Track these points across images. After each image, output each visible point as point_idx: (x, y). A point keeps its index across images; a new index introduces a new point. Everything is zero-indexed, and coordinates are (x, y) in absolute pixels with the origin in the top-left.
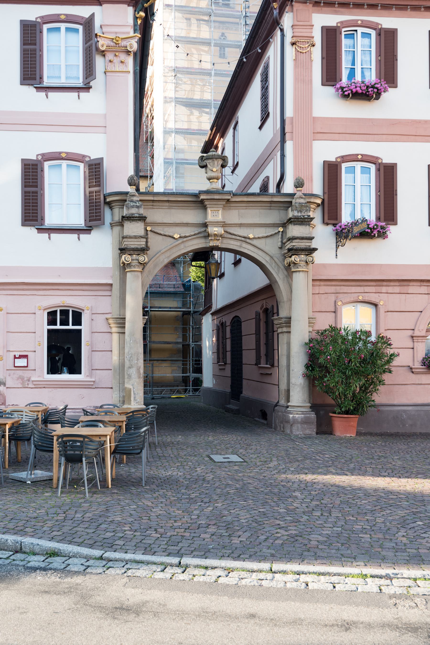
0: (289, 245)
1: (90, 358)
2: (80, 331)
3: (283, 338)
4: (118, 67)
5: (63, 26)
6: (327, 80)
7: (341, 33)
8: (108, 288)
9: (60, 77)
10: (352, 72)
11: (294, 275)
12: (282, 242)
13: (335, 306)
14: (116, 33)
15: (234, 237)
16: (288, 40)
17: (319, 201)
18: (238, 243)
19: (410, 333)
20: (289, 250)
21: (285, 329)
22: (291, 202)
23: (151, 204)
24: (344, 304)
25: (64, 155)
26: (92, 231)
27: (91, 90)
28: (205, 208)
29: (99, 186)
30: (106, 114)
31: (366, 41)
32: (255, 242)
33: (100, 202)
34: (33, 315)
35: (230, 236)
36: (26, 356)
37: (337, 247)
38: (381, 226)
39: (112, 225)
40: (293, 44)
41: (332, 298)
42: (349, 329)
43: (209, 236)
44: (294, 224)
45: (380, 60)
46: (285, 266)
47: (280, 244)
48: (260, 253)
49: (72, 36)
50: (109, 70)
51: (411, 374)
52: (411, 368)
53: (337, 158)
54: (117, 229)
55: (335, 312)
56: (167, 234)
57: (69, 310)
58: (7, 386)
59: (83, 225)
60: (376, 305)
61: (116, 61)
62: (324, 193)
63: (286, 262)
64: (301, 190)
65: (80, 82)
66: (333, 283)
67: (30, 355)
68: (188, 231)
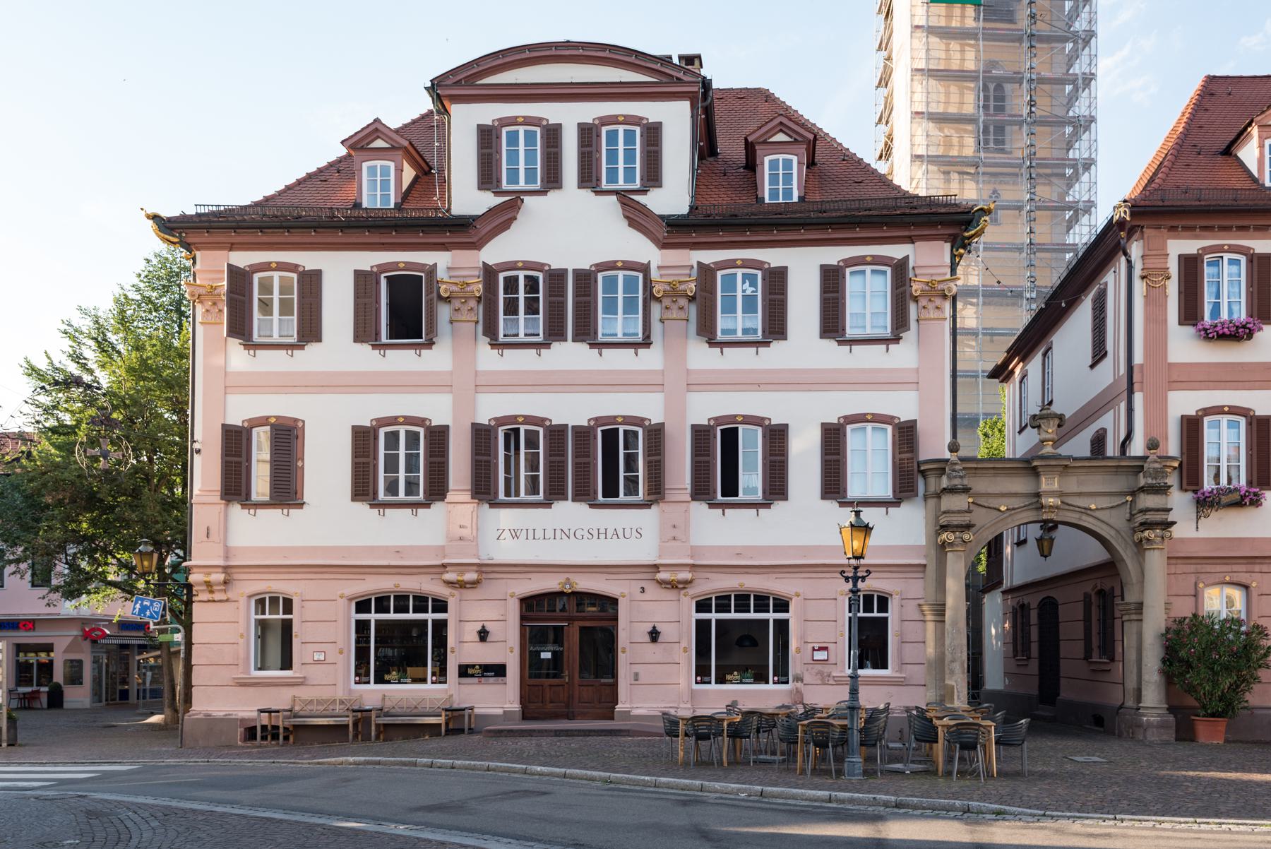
0: (1140, 518)
1: (900, 652)
2: (886, 619)
3: (1131, 629)
4: (933, 314)
5: (868, 269)
6: (1186, 319)
7: (1203, 262)
8: (919, 569)
9: (864, 327)
10: (1216, 308)
11: (1147, 553)
12: (1130, 513)
13: (1196, 588)
14: (932, 275)
15: (1072, 508)
16: (1137, 272)
17: (1176, 464)
18: (1077, 516)
20: (1142, 524)
21: (1134, 617)
22: (1143, 466)
23: (974, 471)
24: (1207, 586)
25: (869, 417)
26: (902, 505)
27: (901, 341)
29: (912, 452)
30: (918, 369)
31: (1234, 269)
32: (1097, 514)
33: (913, 470)
34: (834, 601)
35: (1067, 507)
36: (826, 649)
37: (1198, 518)
38: (1254, 493)
39: (926, 498)
40: (1143, 278)
41: (1192, 579)
42: (1214, 616)
43: (1042, 507)
44: (1148, 494)
45: (1252, 292)
46: (1134, 542)
47: (1128, 515)
48: (1104, 526)
49: (879, 279)
50: (923, 317)
53: (1197, 411)
54: (932, 502)
55: (1195, 596)
56: (991, 505)
58: (805, 682)
59: (891, 497)
60: (1246, 587)
61: (930, 306)
62: (1182, 454)
63: (1135, 538)
64: (1154, 453)
66: (1193, 561)
67: (831, 646)
68: (1015, 502)
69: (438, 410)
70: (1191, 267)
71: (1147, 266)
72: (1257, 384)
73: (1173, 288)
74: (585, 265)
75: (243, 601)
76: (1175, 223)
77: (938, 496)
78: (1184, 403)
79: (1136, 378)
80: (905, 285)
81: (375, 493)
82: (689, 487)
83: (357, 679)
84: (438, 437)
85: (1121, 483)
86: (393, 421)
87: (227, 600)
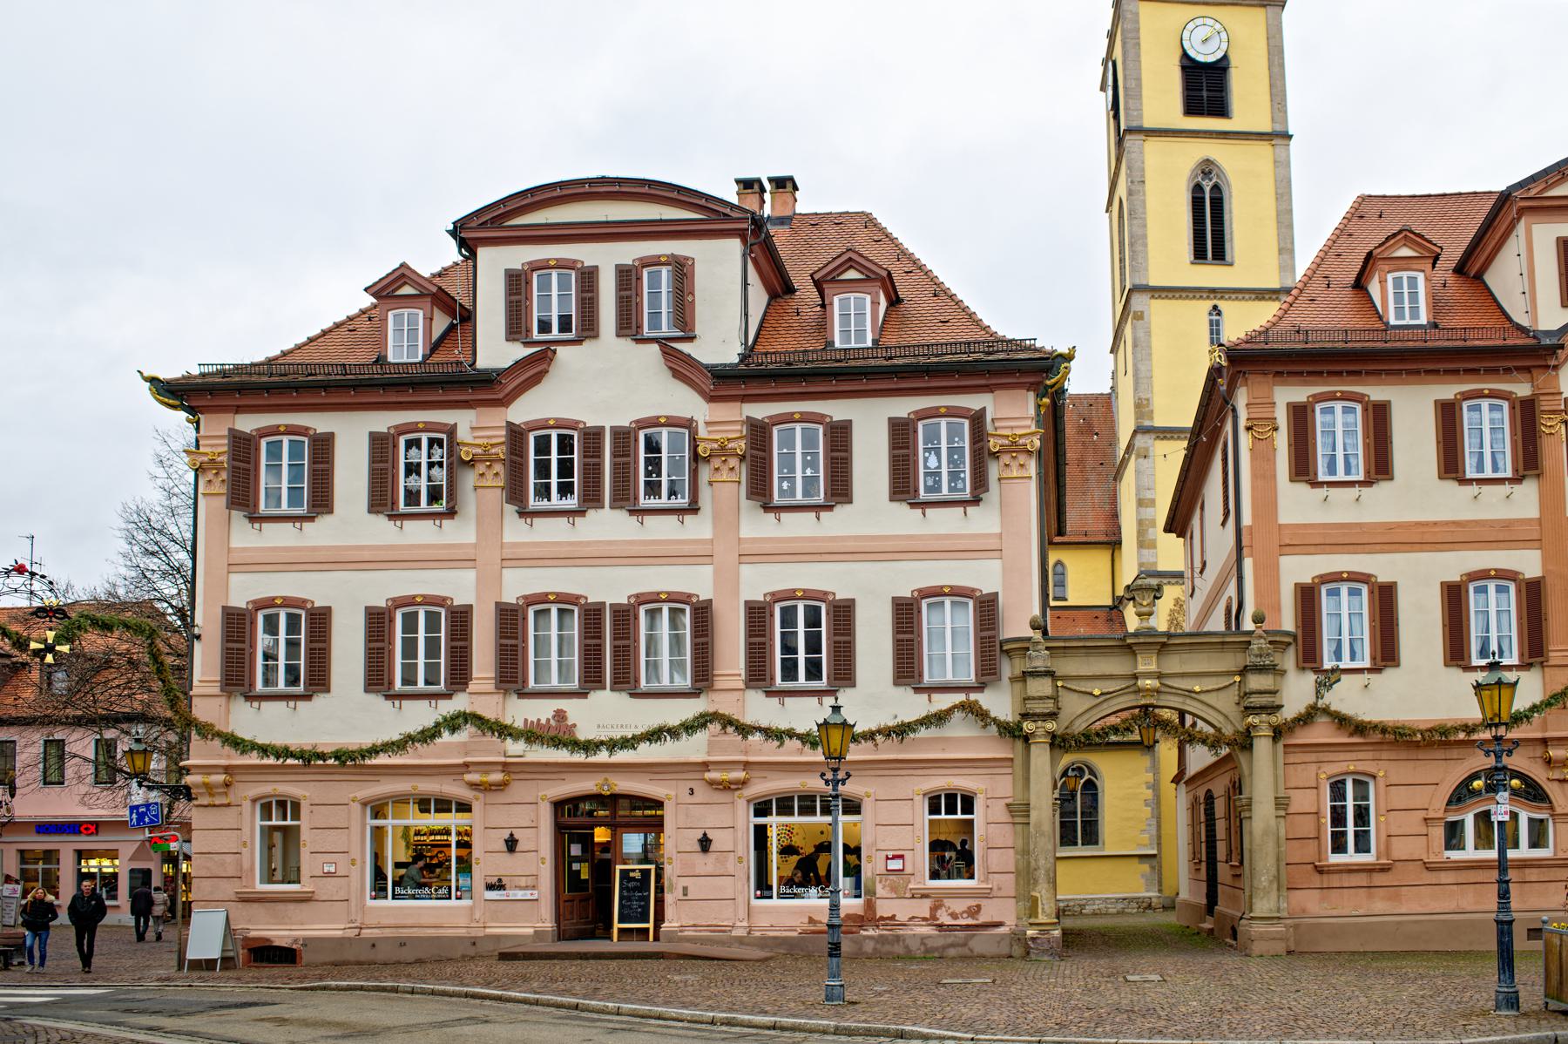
1: (985, 858)
8: (1009, 764)
14: (1012, 428)
15: (1174, 691)
16: (1242, 423)
18: (1181, 700)
19: (1423, 814)
26: (986, 691)
28: (1134, 654)
32: (1202, 697)
36: (901, 857)
39: (1013, 680)
40: (1249, 429)
43: (1139, 691)
47: (1237, 698)
51: (1425, 871)
52: (1425, 863)
53: (1313, 578)
54: (1018, 686)
57: (956, 795)
61: (1014, 464)
62: (1297, 627)
65: (967, 494)
67: (908, 855)
69: (460, 587)
70: (1301, 416)
71: (1252, 416)
72: (1378, 547)
73: (1282, 441)
74: (624, 422)
75: (247, 805)
76: (1280, 369)
77: (1025, 675)
78: (1298, 569)
79: (1245, 541)
80: (982, 440)
81: (391, 683)
82: (743, 672)
83: (759, 893)
84: (461, 619)
85: (1230, 661)
86: (410, 601)
87: (228, 805)
